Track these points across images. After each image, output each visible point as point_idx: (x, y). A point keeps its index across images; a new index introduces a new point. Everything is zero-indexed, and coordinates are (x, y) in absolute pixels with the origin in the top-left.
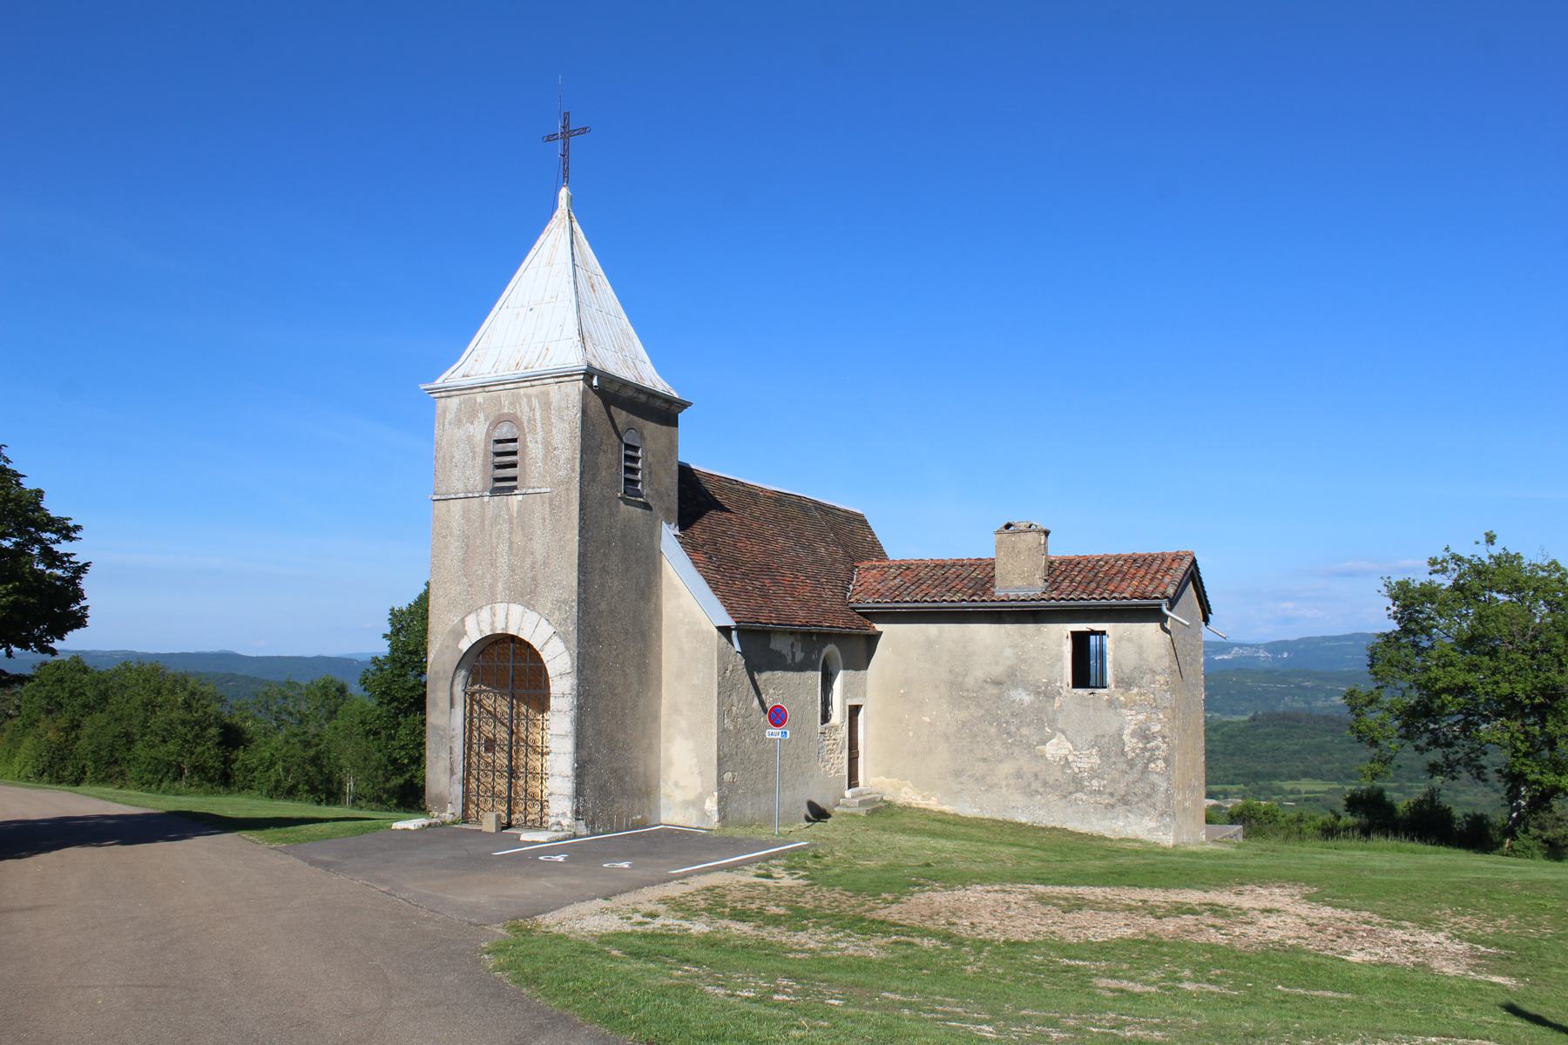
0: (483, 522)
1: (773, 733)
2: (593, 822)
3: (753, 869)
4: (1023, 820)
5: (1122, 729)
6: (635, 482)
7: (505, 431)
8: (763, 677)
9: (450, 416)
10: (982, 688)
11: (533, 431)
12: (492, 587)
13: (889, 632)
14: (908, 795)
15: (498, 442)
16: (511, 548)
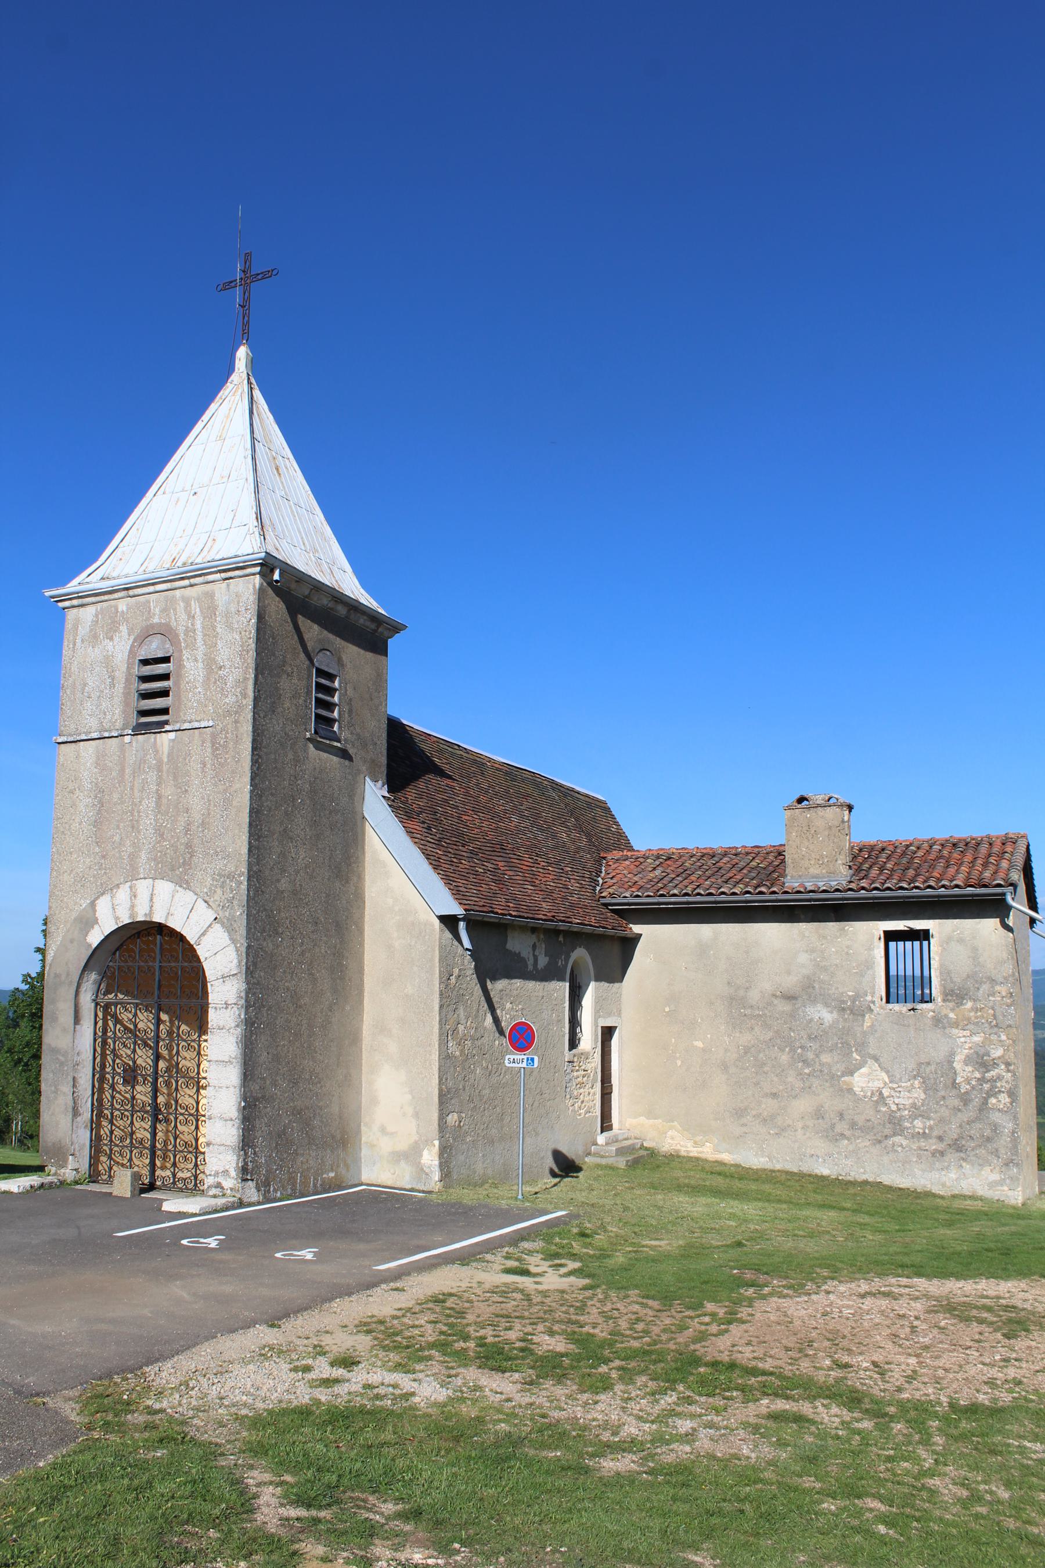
0: (122, 771)
1: (514, 1060)
2: (267, 1184)
3: (497, 1260)
4: (826, 1172)
5: (952, 1054)
6: (330, 722)
7: (154, 648)
8: (496, 987)
9: (83, 631)
10: (770, 1004)
11: (192, 646)
12: (133, 857)
13: (651, 935)
14: (675, 1140)
15: (145, 662)
16: (158, 804)
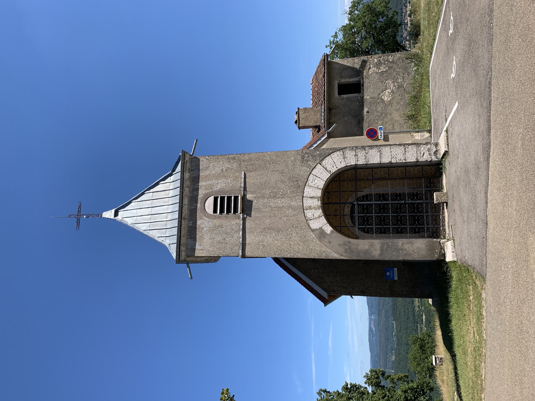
5: (376, 73)
15: (215, 211)
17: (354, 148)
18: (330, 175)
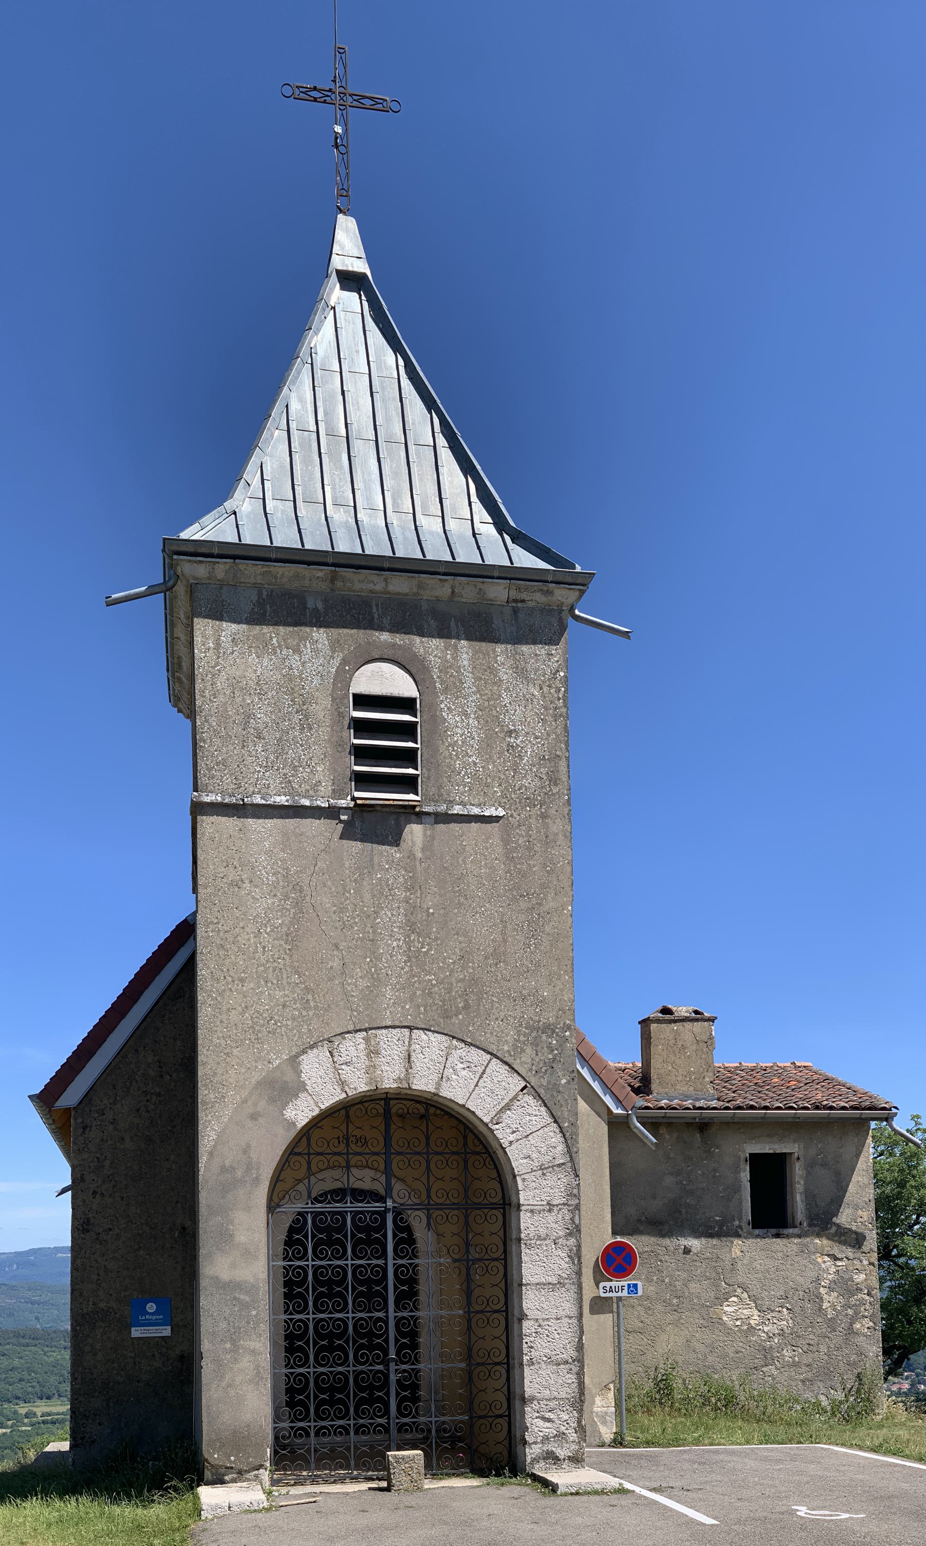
17: (574, 1202)
18: (486, 1119)
